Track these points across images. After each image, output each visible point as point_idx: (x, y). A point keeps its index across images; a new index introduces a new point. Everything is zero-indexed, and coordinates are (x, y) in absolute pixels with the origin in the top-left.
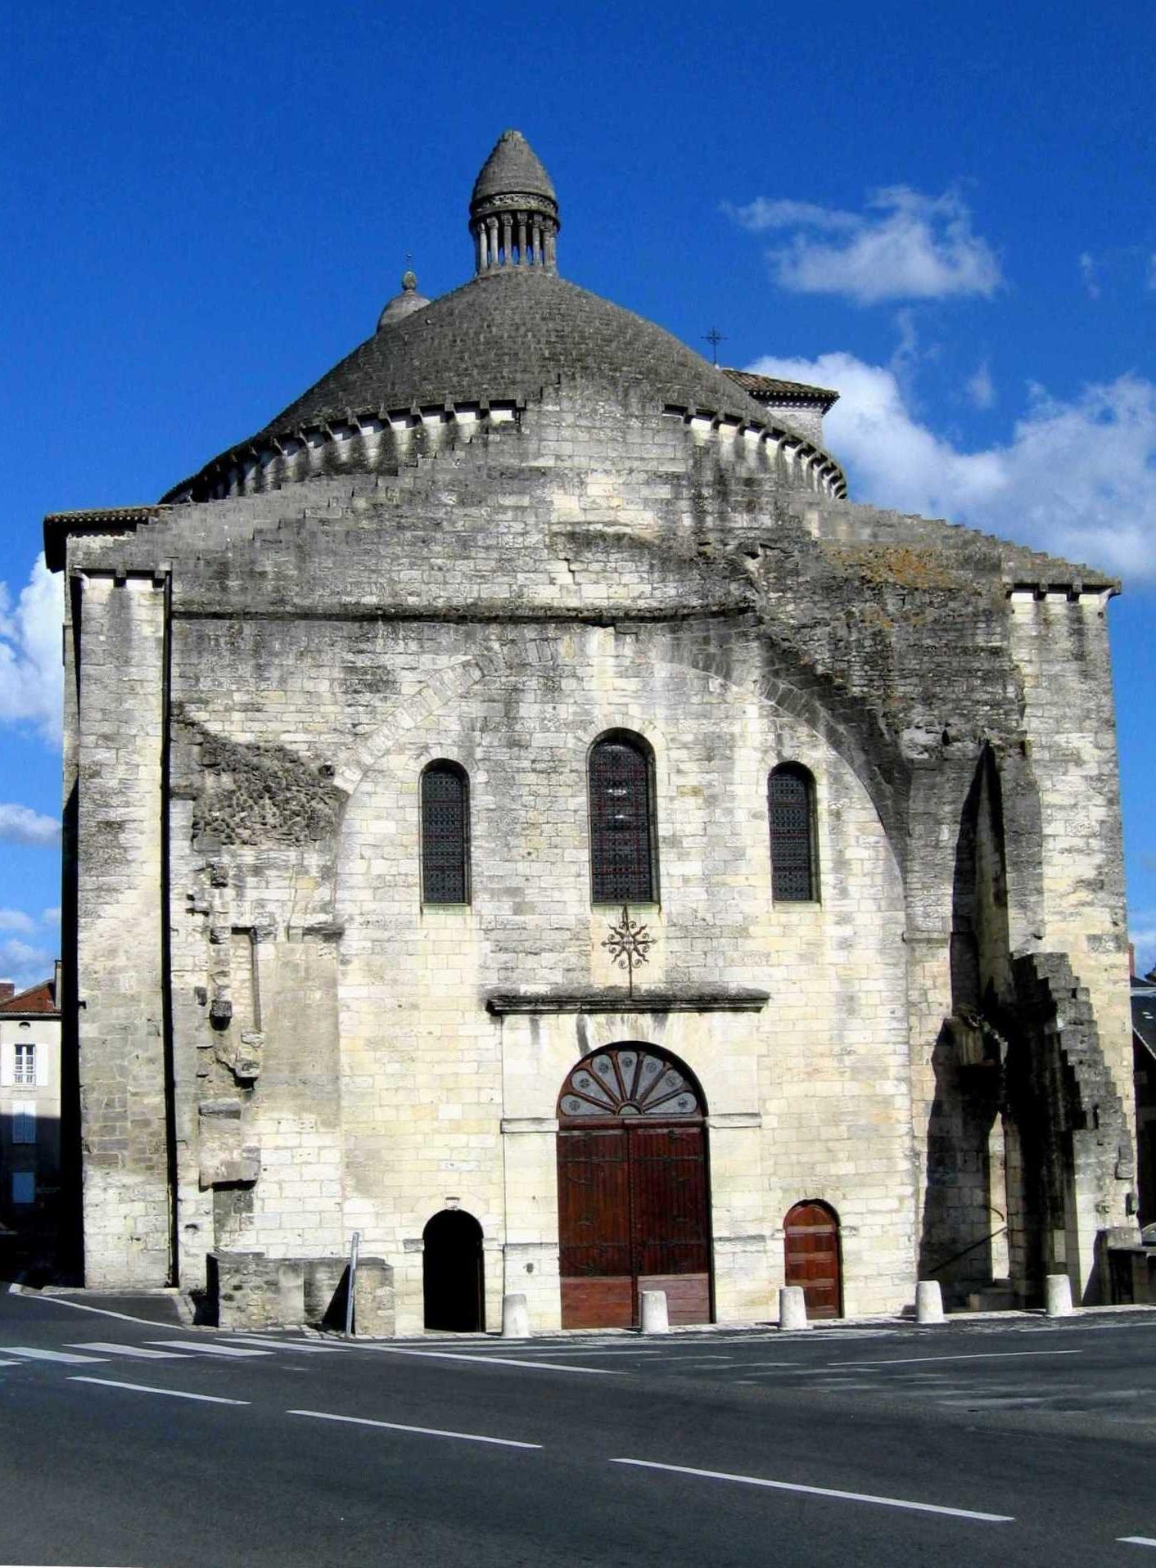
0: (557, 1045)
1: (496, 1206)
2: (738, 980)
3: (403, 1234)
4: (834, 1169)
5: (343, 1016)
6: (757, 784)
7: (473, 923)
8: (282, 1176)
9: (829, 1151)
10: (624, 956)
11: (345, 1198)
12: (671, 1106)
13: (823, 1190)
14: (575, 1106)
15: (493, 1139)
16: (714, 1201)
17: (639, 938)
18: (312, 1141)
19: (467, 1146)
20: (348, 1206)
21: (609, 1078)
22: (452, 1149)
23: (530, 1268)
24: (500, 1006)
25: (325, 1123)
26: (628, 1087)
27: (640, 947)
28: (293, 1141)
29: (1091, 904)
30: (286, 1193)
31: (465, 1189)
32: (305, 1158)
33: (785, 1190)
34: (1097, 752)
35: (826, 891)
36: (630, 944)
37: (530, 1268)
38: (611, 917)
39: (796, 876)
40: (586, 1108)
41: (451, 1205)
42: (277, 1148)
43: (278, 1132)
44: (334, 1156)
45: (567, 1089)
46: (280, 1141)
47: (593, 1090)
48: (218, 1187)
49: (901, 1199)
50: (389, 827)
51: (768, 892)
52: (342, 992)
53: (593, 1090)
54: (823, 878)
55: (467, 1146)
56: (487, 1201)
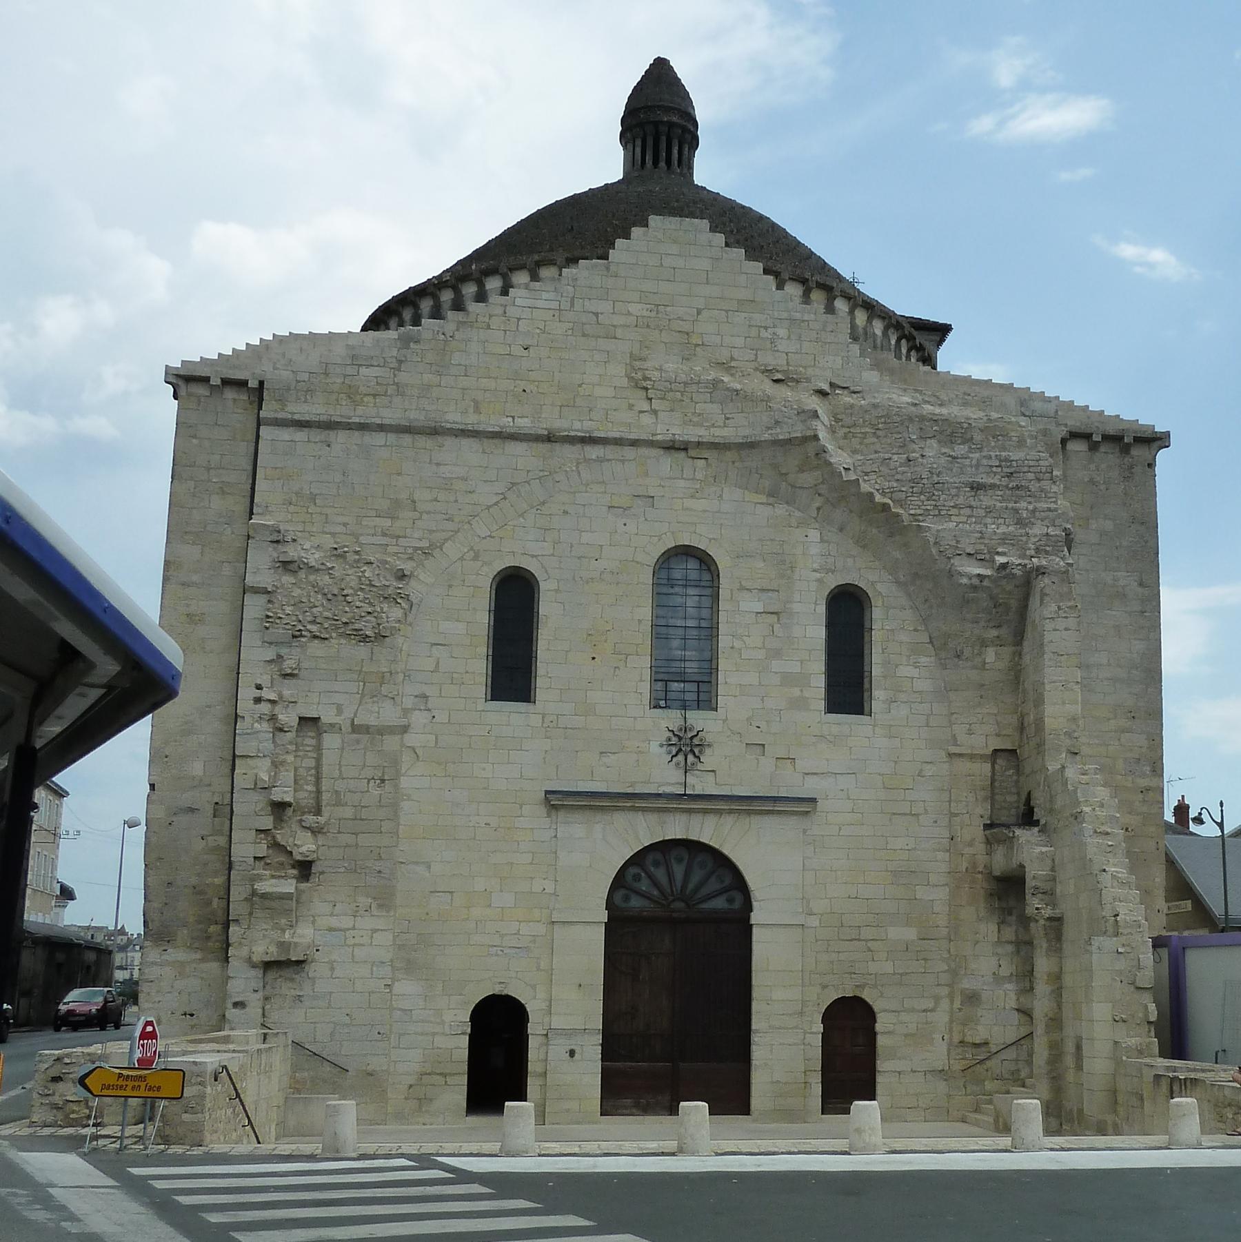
0: (614, 842)
1: (541, 994)
2: (791, 784)
3: (448, 1017)
4: (873, 968)
5: (405, 805)
6: (816, 604)
7: (535, 720)
8: (334, 957)
9: (870, 950)
10: (681, 758)
11: (394, 980)
12: (719, 903)
13: (861, 987)
14: (626, 899)
15: (541, 929)
16: (755, 994)
17: (696, 741)
18: (366, 923)
19: (518, 933)
20: (399, 988)
21: (660, 874)
22: (502, 936)
23: (572, 1053)
24: (558, 801)
25: (380, 906)
26: (679, 883)
27: (696, 751)
28: (347, 922)
29: (1129, 731)
30: (337, 973)
31: (514, 975)
32: (357, 941)
33: (824, 987)
34: (1140, 590)
35: (876, 706)
36: (687, 747)
37: (572, 1053)
38: (671, 719)
39: (847, 689)
40: (636, 902)
41: (497, 990)
42: (331, 930)
43: (332, 915)
44: (385, 939)
45: (619, 882)
46: (334, 922)
47: (644, 885)
48: (268, 966)
49: (937, 999)
50: (461, 628)
51: (822, 705)
52: (404, 782)
53: (644, 885)
54: (876, 693)
55: (518, 933)
56: (534, 987)
